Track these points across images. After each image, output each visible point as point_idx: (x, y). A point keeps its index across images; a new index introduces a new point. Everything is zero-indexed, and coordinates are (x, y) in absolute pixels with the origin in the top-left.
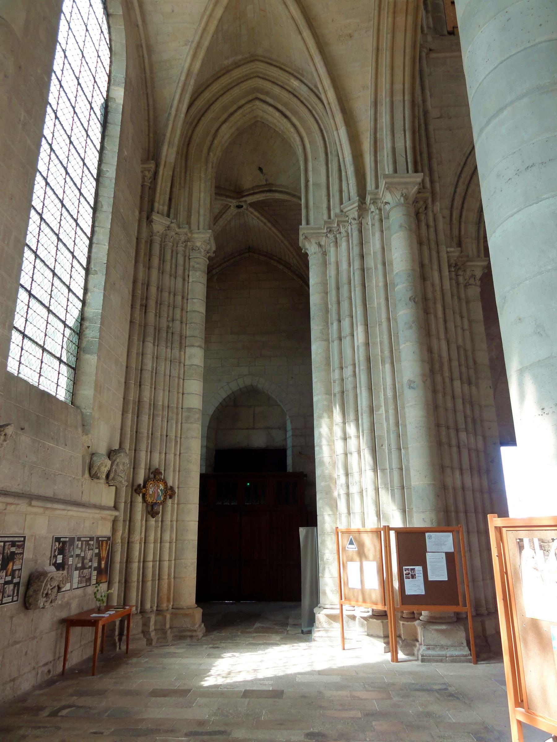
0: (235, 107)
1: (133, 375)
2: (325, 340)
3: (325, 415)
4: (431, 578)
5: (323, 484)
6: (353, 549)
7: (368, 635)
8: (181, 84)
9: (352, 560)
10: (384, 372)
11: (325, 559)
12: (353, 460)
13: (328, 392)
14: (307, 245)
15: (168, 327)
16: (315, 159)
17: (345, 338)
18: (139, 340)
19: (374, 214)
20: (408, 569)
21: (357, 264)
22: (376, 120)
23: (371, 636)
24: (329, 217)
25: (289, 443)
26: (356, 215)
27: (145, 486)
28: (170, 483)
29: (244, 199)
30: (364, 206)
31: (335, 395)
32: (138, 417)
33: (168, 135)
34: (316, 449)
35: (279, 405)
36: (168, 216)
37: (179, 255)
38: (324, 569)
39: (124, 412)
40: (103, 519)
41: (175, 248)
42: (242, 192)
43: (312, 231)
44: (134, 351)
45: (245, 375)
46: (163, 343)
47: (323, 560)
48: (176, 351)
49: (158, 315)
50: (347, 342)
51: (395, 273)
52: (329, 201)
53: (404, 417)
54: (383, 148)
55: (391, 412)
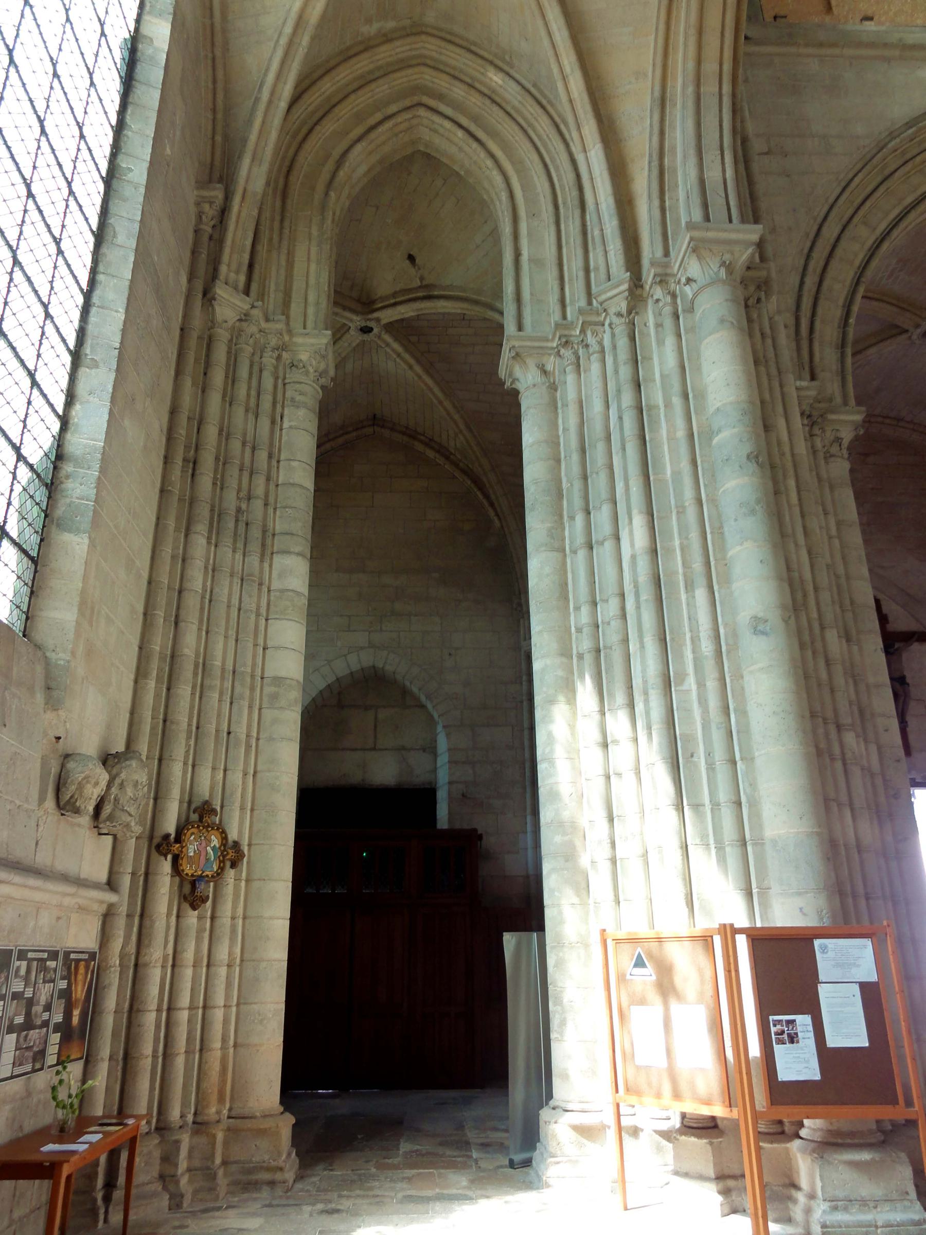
0: (379, 116)
1: (162, 599)
2: (558, 550)
3: (561, 698)
4: (832, 1041)
5: (558, 839)
6: (648, 975)
7: (676, 1173)
8: (283, 41)
9: (642, 1002)
10: (691, 605)
11: (565, 1001)
12: (623, 789)
13: (565, 652)
14: (518, 372)
15: (239, 510)
16: (533, 215)
17: (601, 543)
18: (177, 530)
19: (661, 304)
20: (780, 1021)
21: (627, 399)
22: (662, 133)
23: (686, 1175)
24: (564, 317)
25: (443, 777)
26: (623, 307)
27: (178, 839)
28: (233, 835)
29: (376, 315)
30: (639, 292)
31: (581, 657)
32: (168, 689)
33: (253, 137)
34: (542, 767)
35: (423, 707)
36: (247, 292)
37: (266, 374)
38: (563, 1023)
39: (140, 674)
40: (81, 909)
41: (257, 358)
42: (373, 302)
43: (528, 344)
44: (167, 551)
45: (362, 648)
46: (227, 540)
47: (559, 1002)
48: (254, 560)
49: (220, 484)
50: (605, 552)
51: (712, 410)
52: (562, 289)
53: (741, 694)
54: (677, 186)
55: (712, 685)
